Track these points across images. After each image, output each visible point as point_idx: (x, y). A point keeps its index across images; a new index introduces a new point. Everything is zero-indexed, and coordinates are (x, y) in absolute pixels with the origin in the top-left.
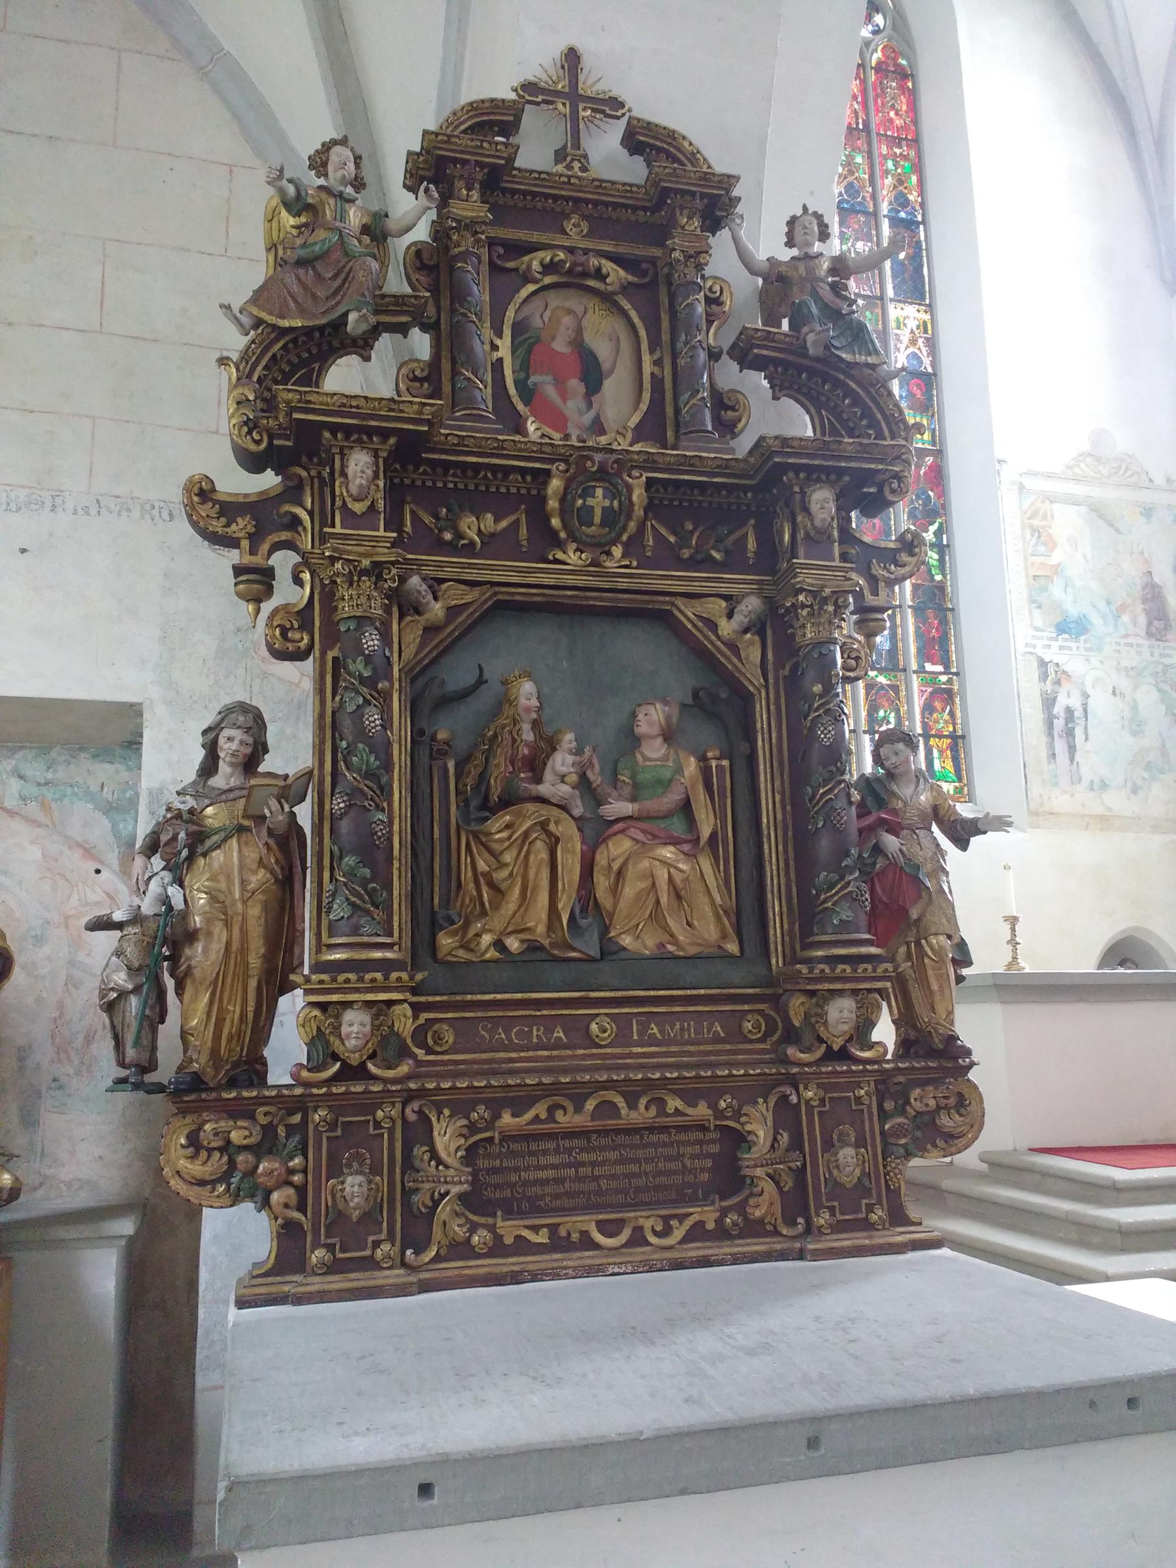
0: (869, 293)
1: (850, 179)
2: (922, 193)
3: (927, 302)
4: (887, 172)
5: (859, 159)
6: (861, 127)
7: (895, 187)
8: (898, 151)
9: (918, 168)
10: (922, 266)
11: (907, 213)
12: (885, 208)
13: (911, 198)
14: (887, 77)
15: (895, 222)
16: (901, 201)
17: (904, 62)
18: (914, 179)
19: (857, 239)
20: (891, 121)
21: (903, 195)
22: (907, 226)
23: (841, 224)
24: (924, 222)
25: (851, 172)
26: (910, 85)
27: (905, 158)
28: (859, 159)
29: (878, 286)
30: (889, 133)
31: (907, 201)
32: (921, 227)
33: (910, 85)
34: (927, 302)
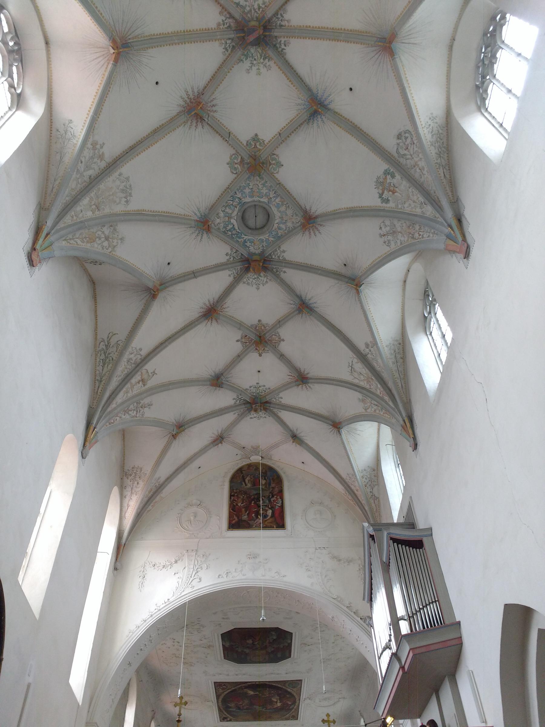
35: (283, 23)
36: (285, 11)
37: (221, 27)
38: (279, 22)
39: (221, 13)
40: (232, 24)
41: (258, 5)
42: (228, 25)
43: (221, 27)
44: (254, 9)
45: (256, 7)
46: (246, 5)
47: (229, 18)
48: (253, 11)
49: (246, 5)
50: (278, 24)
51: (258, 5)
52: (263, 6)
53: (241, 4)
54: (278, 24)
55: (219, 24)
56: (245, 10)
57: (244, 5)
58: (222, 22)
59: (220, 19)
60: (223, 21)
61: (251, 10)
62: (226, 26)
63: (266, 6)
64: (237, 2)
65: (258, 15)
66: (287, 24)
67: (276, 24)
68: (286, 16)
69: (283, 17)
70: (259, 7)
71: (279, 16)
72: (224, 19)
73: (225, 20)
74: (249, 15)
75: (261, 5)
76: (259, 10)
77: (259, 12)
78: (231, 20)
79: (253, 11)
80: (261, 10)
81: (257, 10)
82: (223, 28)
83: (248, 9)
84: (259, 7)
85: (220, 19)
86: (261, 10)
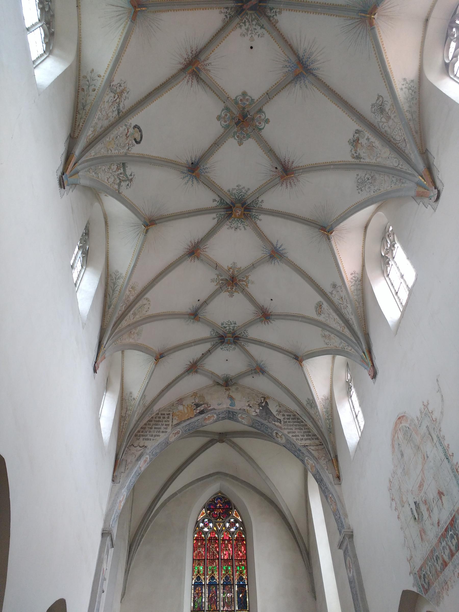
0: (230, 610)
1: (227, 575)
2: (247, 576)
3: (248, 609)
4: (237, 570)
5: (229, 568)
6: (230, 558)
7: (239, 575)
8: (240, 563)
9: (246, 568)
10: (247, 598)
11: (242, 582)
12: (236, 582)
13: (244, 577)
14: (238, 542)
15: (239, 586)
16: (241, 579)
17: (243, 536)
18: (245, 571)
19: (227, 593)
20: (239, 555)
21: (242, 577)
22: (242, 587)
23: (223, 589)
24: (247, 584)
25: (227, 573)
26: (245, 542)
27: (242, 565)
28: (229, 568)
29: (233, 607)
30: (238, 558)
31: (243, 578)
32: (247, 586)
33: (245, 542)
34: (248, 609)
35: (226, 10)
36: (224, 20)
37: (278, 10)
38: (229, 11)
39: (277, 22)
40: (269, 11)
41: (245, 25)
42: (272, 11)
43: (278, 10)
44: (249, 22)
45: (247, 24)
46: (255, 26)
47: (270, 17)
48: (250, 20)
49: (255, 26)
50: (230, 9)
51: (245, 25)
52: (241, 24)
53: (259, 27)
54: (230, 9)
55: (280, 12)
56: (256, 21)
57: (257, 26)
58: (277, 14)
59: (278, 17)
60: (276, 15)
61: (252, 21)
62: (274, 10)
63: (239, 24)
64: (262, 29)
65: (246, 17)
66: (222, 10)
67: (231, 9)
68: (223, 16)
69: (226, 16)
70: (245, 23)
71: (228, 16)
72: (275, 17)
73: (274, 15)
74: (254, 17)
75: (243, 25)
76: (245, 21)
77: (245, 19)
78: (269, 14)
79: (250, 20)
80: (243, 21)
81: (247, 21)
82: (277, 9)
83: (254, 23)
84: (245, 23)
85: (278, 17)
86: (243, 21)
